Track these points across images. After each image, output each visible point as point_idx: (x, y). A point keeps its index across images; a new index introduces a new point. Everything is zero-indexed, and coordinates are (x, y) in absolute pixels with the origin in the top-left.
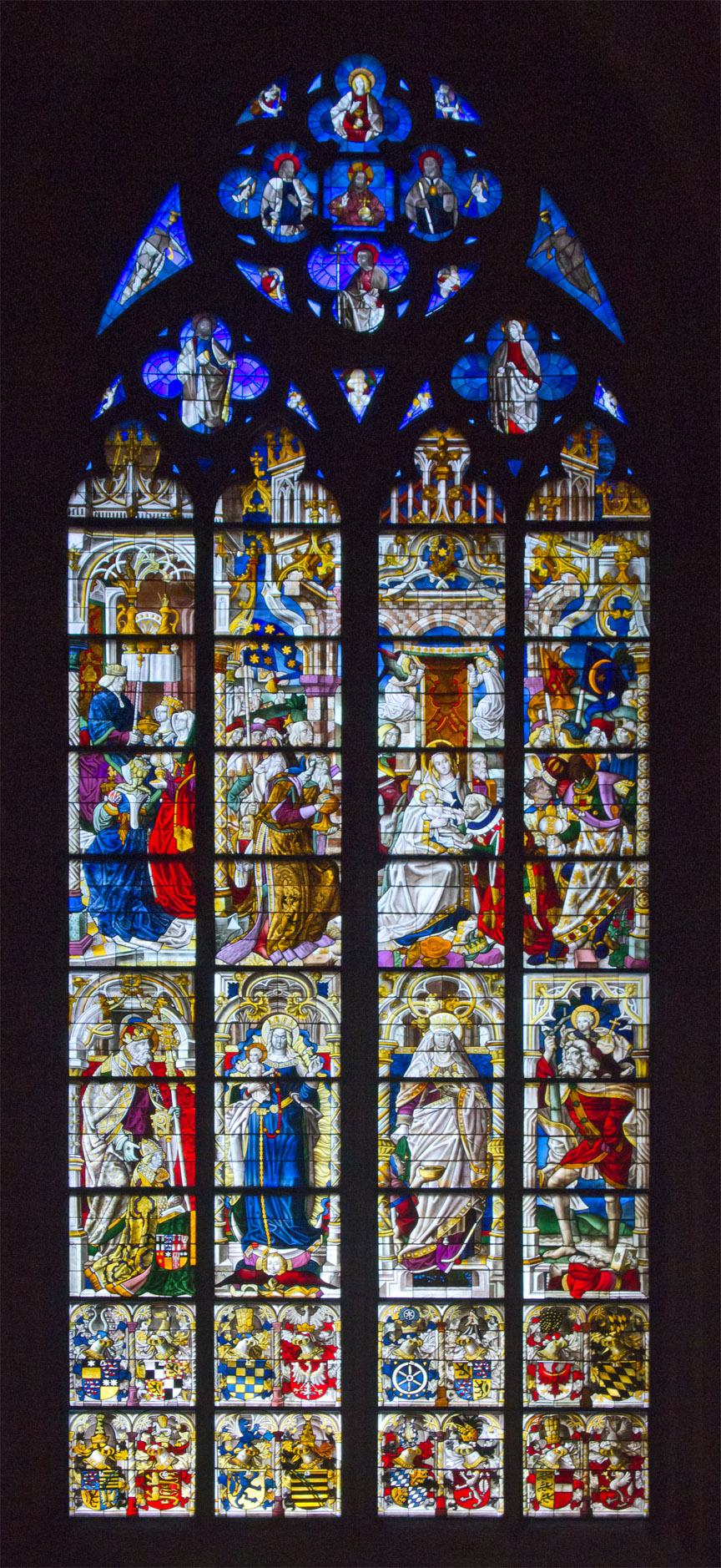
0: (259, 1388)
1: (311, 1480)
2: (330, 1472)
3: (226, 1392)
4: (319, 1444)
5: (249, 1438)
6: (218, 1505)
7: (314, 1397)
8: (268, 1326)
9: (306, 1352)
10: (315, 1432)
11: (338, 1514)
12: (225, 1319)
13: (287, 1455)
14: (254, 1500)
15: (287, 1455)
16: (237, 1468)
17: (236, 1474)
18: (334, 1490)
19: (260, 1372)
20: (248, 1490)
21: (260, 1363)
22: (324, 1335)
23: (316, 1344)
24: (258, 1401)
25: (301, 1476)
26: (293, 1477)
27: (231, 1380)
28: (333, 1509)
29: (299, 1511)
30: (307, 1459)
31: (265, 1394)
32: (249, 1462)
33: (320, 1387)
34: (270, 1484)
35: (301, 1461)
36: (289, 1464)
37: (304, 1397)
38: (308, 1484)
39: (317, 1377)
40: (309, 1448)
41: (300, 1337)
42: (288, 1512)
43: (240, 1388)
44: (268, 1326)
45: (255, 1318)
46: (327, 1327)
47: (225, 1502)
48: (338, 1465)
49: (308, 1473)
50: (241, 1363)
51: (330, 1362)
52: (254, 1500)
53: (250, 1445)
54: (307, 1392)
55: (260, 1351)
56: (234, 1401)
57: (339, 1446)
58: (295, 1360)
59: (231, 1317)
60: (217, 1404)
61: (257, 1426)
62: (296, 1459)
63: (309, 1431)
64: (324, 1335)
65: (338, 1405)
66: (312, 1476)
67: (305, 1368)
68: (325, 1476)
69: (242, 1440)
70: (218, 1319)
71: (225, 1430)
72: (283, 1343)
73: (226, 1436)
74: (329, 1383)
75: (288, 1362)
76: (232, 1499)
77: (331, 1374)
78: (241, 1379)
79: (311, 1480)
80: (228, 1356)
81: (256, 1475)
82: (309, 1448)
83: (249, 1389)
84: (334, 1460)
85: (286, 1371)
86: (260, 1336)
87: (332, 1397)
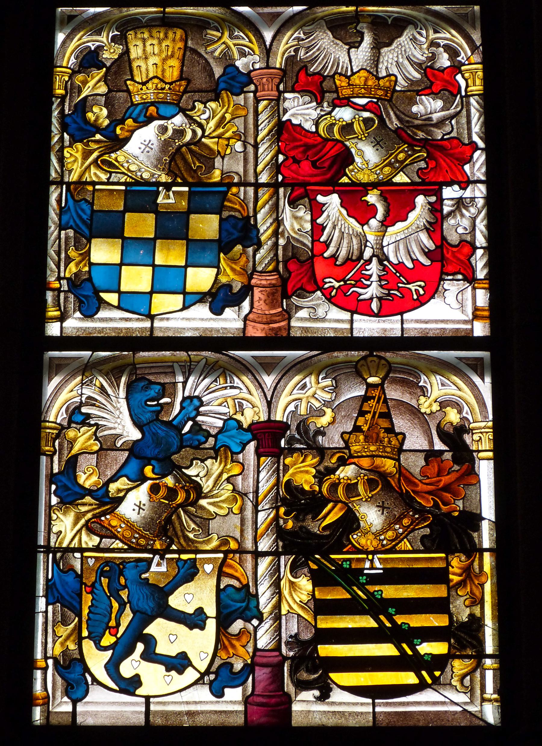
0: (201, 279)
1: (390, 592)
2: (457, 563)
3: (87, 294)
4: (415, 464)
5: (165, 447)
6: (45, 681)
7: (395, 303)
8: (236, 82)
9: (367, 156)
10: (401, 423)
11: (490, 714)
12: (90, 60)
13: (295, 501)
14: (179, 663)
15: (295, 501)
16: (117, 550)
17: (112, 570)
18: (475, 624)
19: (206, 226)
20: (158, 628)
21: (208, 196)
22: (430, 106)
23: (400, 134)
24: (199, 320)
25: (350, 576)
26: (320, 579)
27: (104, 252)
28: (469, 695)
29: (344, 704)
30: (372, 516)
31: (219, 298)
32: (163, 528)
33: (416, 272)
34: (236, 605)
35: (350, 522)
36: (309, 537)
37: (359, 307)
38: (376, 607)
39: (405, 239)
40: (378, 480)
41: (345, 114)
42: (306, 707)
43: (136, 279)
44: (236, 82)
45: (190, 56)
46: (437, 81)
47: (74, 675)
48: (486, 537)
49: (377, 565)
50: (140, 196)
51: (450, 193)
52: (179, 663)
53: (168, 466)
54: (372, 291)
55: (208, 158)
56: (112, 320)
57: (486, 470)
58: (331, 185)
59: (109, 55)
60: (53, 330)
61: (194, 403)
62: (333, 515)
63: (377, 423)
64: (430, 106)
65: (480, 329)
66: (392, 576)
67: (363, 213)
68: (439, 576)
69: (133, 449)
70: (68, 59)
71: (77, 416)
72: (283, 130)
73: (82, 438)
74: (446, 260)
75: (303, 193)
76: (96, 661)
77: (455, 228)
78: (138, 250)
79: (390, 592)
80: (97, 174)
81: (188, 573)
82: (378, 480)
83: (166, 281)
84: (473, 520)
85: (296, 221)
86: (209, 113)
87: (454, 308)
